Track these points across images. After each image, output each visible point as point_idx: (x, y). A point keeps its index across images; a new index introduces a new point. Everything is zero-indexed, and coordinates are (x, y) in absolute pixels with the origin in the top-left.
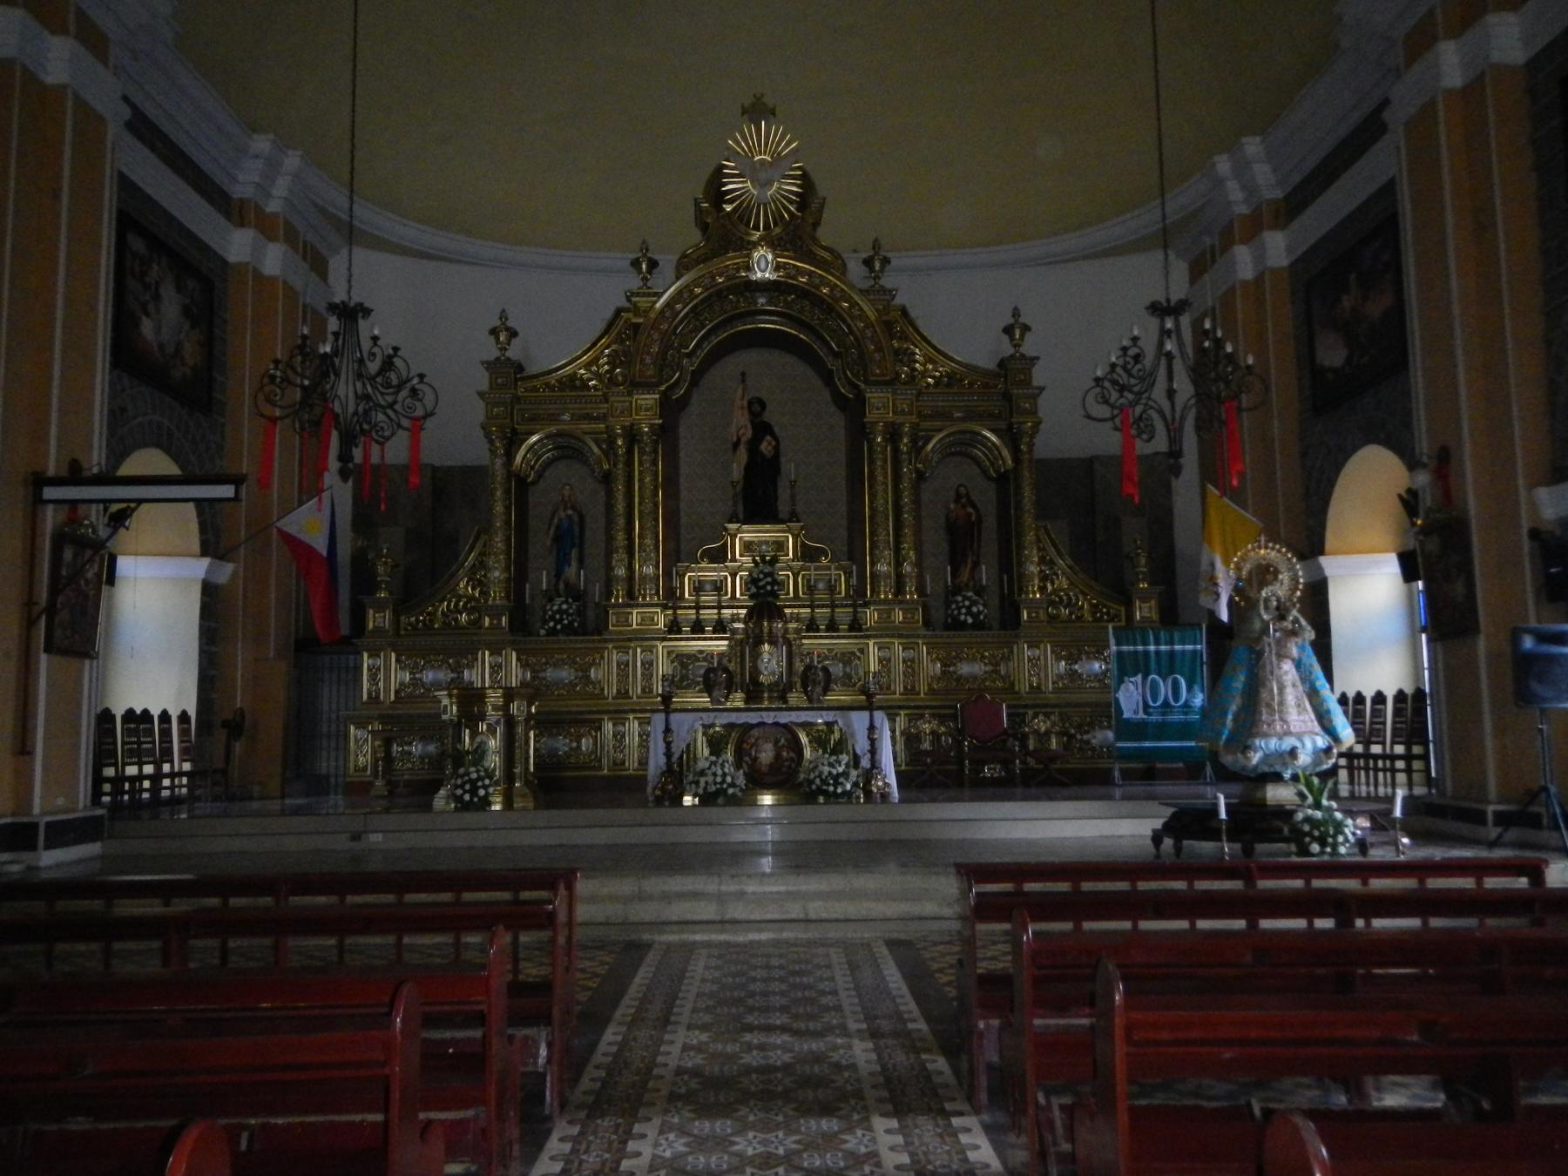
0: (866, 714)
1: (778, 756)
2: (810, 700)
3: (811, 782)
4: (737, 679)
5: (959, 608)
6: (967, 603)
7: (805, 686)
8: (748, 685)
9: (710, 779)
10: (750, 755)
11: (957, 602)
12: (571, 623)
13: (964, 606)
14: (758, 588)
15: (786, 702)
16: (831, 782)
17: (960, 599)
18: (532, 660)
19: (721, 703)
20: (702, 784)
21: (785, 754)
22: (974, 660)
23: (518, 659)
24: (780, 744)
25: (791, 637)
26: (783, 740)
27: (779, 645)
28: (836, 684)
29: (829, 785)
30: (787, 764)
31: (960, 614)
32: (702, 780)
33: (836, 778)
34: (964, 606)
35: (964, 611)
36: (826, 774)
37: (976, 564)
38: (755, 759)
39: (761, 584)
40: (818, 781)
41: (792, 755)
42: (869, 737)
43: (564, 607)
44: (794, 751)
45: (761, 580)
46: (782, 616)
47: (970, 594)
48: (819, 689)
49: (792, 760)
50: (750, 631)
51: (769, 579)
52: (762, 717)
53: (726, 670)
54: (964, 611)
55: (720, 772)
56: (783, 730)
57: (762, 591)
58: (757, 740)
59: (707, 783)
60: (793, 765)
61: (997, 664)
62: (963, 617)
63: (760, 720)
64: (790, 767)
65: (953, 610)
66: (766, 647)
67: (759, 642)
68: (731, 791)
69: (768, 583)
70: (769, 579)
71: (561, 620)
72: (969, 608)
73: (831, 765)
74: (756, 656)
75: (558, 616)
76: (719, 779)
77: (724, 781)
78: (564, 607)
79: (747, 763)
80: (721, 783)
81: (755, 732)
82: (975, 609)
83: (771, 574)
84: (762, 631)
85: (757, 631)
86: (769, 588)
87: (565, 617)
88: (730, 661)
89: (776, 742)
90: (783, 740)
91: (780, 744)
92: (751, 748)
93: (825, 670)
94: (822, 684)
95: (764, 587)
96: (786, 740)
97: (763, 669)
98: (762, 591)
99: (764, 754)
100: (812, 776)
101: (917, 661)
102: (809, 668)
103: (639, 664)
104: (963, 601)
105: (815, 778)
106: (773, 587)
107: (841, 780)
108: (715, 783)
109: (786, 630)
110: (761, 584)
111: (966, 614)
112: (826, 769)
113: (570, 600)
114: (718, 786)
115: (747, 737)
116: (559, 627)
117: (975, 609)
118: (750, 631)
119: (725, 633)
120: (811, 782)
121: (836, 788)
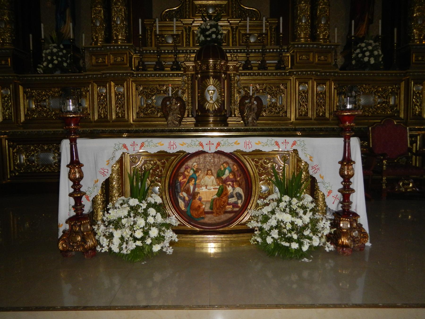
0: (340, 141)
1: (222, 193)
2: (246, 124)
3: (264, 234)
4: (189, 107)
5: (363, 52)
6: (370, 48)
7: (242, 112)
8: (197, 111)
9: (127, 233)
10: (187, 191)
11: (361, 48)
12: (60, 63)
13: (367, 50)
14: (206, 36)
15: (227, 125)
16: (295, 237)
17: (363, 45)
18: (35, 92)
19: (177, 126)
20: (116, 241)
21: (230, 189)
22: (370, 93)
23: (25, 92)
24: (224, 177)
25: (231, 73)
26: (227, 172)
27: (222, 80)
28: (265, 111)
29: (290, 240)
30: (231, 200)
31: (364, 56)
32: (117, 234)
33: (300, 230)
34: (367, 50)
35: (367, 54)
36: (289, 226)
37: (371, 22)
38: (193, 195)
39: (207, 33)
40: (275, 234)
41: (238, 190)
42: (342, 174)
43: (55, 50)
44: (240, 186)
45: (208, 30)
46: (224, 57)
47: (371, 41)
48: (253, 115)
49: (239, 196)
50: (198, 68)
51: (214, 29)
52: (201, 144)
53: (179, 99)
54: (367, 54)
55: (141, 222)
56: (230, 161)
57: (209, 39)
58: (195, 172)
59: (122, 238)
60: (240, 203)
61: (387, 97)
62: (366, 59)
63: (201, 149)
64: (235, 205)
65: (358, 54)
66: (211, 80)
67: (205, 77)
68: (156, 248)
69: (213, 33)
70: (214, 29)
71: (52, 60)
72: (371, 52)
73: (293, 213)
74: (203, 88)
75: (49, 58)
76: (139, 234)
77: (146, 233)
78: (55, 50)
79: (184, 199)
80: (143, 239)
81: (193, 163)
82: (376, 53)
83: (216, 26)
84: (208, 68)
85: (204, 67)
86: (214, 36)
87: (55, 58)
88: (183, 93)
89: (219, 177)
90: (227, 172)
91: (224, 177)
92: (189, 182)
93: (258, 99)
94: (256, 111)
95: (210, 36)
96: (231, 172)
97: (209, 99)
98: (209, 39)
99: (204, 189)
100: (266, 227)
101: (328, 94)
102: (246, 96)
103: (113, 95)
104: (366, 47)
105: (272, 228)
106: (217, 35)
107: (307, 233)
108: (135, 239)
109: (228, 67)
110: (207, 33)
111: (370, 57)
112: (287, 218)
113: (62, 46)
114: (139, 243)
115: (182, 170)
116: (50, 66)
117: (376, 53)
118: (198, 68)
119: (180, 70)
120: (264, 234)
121: (301, 244)
